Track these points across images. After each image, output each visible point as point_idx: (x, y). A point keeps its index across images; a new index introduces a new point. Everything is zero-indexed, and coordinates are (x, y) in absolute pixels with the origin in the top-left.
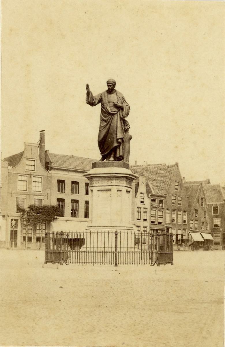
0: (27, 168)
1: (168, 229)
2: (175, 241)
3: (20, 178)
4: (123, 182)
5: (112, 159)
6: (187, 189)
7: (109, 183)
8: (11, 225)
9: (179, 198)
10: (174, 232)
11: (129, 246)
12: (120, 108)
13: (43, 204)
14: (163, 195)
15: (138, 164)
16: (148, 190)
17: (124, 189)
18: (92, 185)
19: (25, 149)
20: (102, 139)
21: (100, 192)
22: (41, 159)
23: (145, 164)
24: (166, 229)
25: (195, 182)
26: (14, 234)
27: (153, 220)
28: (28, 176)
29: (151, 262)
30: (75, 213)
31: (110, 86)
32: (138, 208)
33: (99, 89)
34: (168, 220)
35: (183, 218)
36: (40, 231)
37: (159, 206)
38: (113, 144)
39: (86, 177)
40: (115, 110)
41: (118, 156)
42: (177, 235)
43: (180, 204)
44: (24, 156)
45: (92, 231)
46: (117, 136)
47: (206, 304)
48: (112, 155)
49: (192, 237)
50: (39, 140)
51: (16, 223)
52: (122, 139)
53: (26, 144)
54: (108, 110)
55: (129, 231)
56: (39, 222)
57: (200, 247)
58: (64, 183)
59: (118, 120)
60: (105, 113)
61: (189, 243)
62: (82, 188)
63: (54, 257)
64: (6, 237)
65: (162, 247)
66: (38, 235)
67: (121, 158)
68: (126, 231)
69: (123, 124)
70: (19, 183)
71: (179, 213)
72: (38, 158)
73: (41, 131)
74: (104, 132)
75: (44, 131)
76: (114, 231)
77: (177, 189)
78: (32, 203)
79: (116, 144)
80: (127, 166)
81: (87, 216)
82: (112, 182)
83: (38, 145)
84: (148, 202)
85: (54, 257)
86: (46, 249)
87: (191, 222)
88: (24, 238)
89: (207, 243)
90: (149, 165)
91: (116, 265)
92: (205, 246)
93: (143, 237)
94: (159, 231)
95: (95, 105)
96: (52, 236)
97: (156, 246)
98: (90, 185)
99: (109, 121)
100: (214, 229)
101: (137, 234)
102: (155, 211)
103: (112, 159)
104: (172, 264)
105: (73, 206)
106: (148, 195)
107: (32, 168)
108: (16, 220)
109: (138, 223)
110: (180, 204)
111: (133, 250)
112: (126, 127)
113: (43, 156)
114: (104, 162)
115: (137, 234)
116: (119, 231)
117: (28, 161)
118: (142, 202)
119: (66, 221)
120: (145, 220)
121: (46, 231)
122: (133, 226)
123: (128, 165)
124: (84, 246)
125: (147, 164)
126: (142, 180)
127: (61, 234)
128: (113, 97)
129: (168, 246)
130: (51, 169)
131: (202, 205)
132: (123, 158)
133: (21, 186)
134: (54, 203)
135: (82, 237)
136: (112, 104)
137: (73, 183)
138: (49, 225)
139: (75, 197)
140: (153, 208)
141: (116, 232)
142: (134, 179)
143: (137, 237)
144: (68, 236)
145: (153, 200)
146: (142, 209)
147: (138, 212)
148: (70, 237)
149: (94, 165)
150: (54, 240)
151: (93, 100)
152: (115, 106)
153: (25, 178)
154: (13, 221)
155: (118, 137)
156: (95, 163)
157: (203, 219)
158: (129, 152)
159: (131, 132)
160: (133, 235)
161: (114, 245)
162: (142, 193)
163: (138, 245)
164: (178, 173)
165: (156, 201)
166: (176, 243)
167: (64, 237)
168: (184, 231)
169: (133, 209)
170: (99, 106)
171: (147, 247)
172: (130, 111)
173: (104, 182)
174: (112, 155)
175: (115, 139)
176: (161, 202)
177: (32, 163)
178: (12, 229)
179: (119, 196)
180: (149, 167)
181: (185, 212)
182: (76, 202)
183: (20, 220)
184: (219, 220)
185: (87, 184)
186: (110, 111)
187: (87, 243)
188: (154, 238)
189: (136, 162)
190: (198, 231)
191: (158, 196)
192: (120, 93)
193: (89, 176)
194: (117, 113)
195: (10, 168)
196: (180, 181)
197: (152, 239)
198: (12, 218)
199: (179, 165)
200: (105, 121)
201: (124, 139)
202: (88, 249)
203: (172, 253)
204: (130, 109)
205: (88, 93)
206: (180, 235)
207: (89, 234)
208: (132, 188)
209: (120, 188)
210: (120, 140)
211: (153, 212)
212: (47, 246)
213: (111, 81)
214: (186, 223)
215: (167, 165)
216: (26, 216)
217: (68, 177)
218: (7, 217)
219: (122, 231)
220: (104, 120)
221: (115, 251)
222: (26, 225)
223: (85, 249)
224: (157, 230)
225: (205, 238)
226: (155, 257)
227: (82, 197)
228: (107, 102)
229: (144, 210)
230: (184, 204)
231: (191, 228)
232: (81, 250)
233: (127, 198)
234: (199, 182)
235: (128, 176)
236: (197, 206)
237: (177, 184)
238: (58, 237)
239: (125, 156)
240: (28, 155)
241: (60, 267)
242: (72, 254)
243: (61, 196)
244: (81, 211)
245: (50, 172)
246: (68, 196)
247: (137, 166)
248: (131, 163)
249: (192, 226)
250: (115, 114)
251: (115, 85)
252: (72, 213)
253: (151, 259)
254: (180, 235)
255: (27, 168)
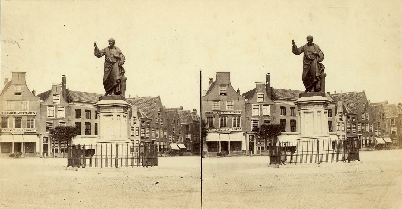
0: (54, 101)
1: (153, 141)
2: (159, 150)
3: (49, 108)
4: (121, 109)
5: (113, 94)
6: (166, 113)
7: (111, 111)
8: (43, 141)
9: (161, 120)
10: (158, 143)
11: (126, 154)
12: (119, 59)
13: (66, 126)
14: (150, 118)
15: (131, 97)
16: (139, 115)
17: (122, 115)
18: (100, 112)
19: (52, 88)
20: (106, 81)
21: (105, 117)
22: (63, 95)
23: (136, 97)
24: (152, 142)
25: (172, 109)
26: (45, 147)
27: (143, 135)
28: (54, 106)
29: (142, 165)
30: (88, 132)
31: (111, 43)
32: (132, 127)
33: (103, 45)
34: (154, 135)
35: (164, 134)
36: (64, 144)
37: (147, 126)
38: (113, 83)
39: (96, 106)
40: (116, 60)
41: (117, 91)
42: (160, 146)
43: (162, 124)
44: (52, 93)
45: (100, 144)
46: (116, 78)
47: (182, 193)
48: (113, 92)
49: (171, 147)
50: (62, 81)
51: (47, 140)
52: (120, 80)
53: (53, 84)
55: (126, 144)
56: (63, 139)
57: (177, 154)
58: (81, 112)
60: (108, 62)
61: (169, 151)
62: (93, 114)
63: (74, 163)
64: (40, 150)
65: (149, 154)
66: (62, 148)
67: (120, 93)
68: (124, 144)
69: (120, 70)
70: (48, 111)
71: (161, 130)
72: (61, 94)
73: (63, 76)
74: (107, 75)
75: (65, 75)
76: (116, 144)
77: (160, 114)
78: (58, 125)
79: (116, 84)
80: (124, 99)
81: (96, 133)
82: (114, 110)
83: (61, 85)
84: (139, 123)
85: (74, 163)
86: (68, 157)
87: (170, 136)
88: (53, 150)
89: (182, 151)
90: (139, 98)
91: (117, 167)
92: (181, 152)
93: (136, 148)
94: (147, 143)
95: (101, 57)
96: (72, 148)
97: (145, 153)
98: (98, 113)
99: (111, 68)
100: (186, 142)
101: (132, 146)
102: (144, 130)
103: (113, 94)
104: (157, 166)
105: (86, 127)
106: (139, 119)
107: (58, 101)
108: (47, 138)
109: (133, 138)
110: (162, 124)
111: (129, 157)
112: (122, 72)
113: (65, 92)
114: (108, 96)
115: (132, 146)
116: (119, 144)
117: (55, 96)
118: (135, 123)
119: (82, 137)
120: (137, 136)
121: (68, 145)
122: (129, 140)
123: (125, 98)
124: (95, 154)
125: (138, 97)
126: (134, 108)
127: (79, 146)
128: (113, 50)
129: (153, 153)
130: (71, 102)
131: (178, 125)
132: (121, 93)
133: (50, 114)
134: (73, 125)
135: (93, 148)
136: (112, 56)
137: (86, 111)
138: (70, 141)
139: (88, 121)
140: (142, 127)
141: (117, 144)
142: (129, 107)
143: (131, 148)
144: (83, 148)
145: (143, 122)
146: (135, 128)
147: (132, 130)
148: (85, 149)
149: (101, 98)
150: (74, 150)
151: (99, 53)
152: (115, 57)
153: (53, 108)
154: (45, 138)
155: (117, 79)
156: (101, 97)
157: (178, 134)
158: (125, 89)
159: (126, 75)
160: (129, 146)
162: (134, 117)
163: (133, 153)
164: (160, 102)
165: (145, 122)
166: (159, 152)
167: (81, 148)
168: (165, 143)
169: (129, 128)
170: (103, 58)
171: (138, 154)
172: (125, 61)
173: (107, 110)
174: (113, 92)
175: (115, 80)
176: (148, 123)
177: (58, 98)
178: (44, 144)
179: (118, 120)
180: (139, 99)
181: (165, 129)
182: (88, 124)
183: (49, 137)
184: (190, 135)
185: (96, 112)
186: (111, 61)
187: (97, 152)
188: (143, 148)
189: (130, 95)
190: (175, 143)
191: (147, 119)
192: (118, 48)
193: (97, 106)
194: (116, 62)
195: (42, 101)
196: (161, 108)
197: (142, 149)
198: (44, 136)
199: (161, 97)
200: (108, 68)
201: (121, 80)
202: (98, 157)
203: (157, 158)
204: (125, 59)
205: (96, 49)
206: (162, 145)
207: (98, 146)
208: (127, 114)
209: (119, 114)
210: (118, 81)
211: (143, 130)
212: (69, 155)
213: (112, 40)
214: (167, 137)
215: (152, 97)
216: (53, 134)
217: (83, 107)
218: (40, 136)
219: (121, 144)
220: (107, 67)
221: (116, 157)
222: (54, 141)
223: (95, 157)
224: (146, 143)
225: (180, 148)
226: (145, 161)
227: (92, 121)
228: (109, 55)
229: (136, 129)
230: (164, 124)
231: (170, 141)
232: (93, 157)
233: (124, 121)
234: (175, 109)
235: (125, 105)
236: (174, 126)
237: (159, 110)
238: (77, 148)
239: (122, 92)
240: (55, 92)
241: (79, 169)
242: (87, 161)
243: (78, 120)
244: (93, 130)
245: (70, 103)
246: (83, 121)
247: (131, 99)
248: (127, 96)
249: (170, 139)
250: (115, 62)
251: (115, 42)
252: (86, 132)
253: (142, 162)
254: (162, 145)
255: (54, 101)
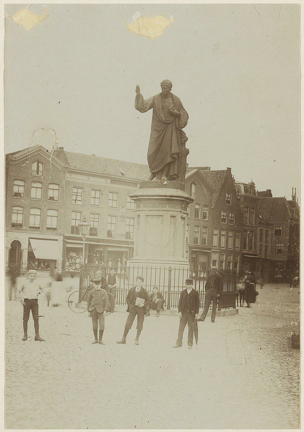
48: (165, 173)
52: (178, 154)
54: (161, 118)
59: (173, 137)
161: (167, 284)
201: (180, 154)
219: (177, 267)
